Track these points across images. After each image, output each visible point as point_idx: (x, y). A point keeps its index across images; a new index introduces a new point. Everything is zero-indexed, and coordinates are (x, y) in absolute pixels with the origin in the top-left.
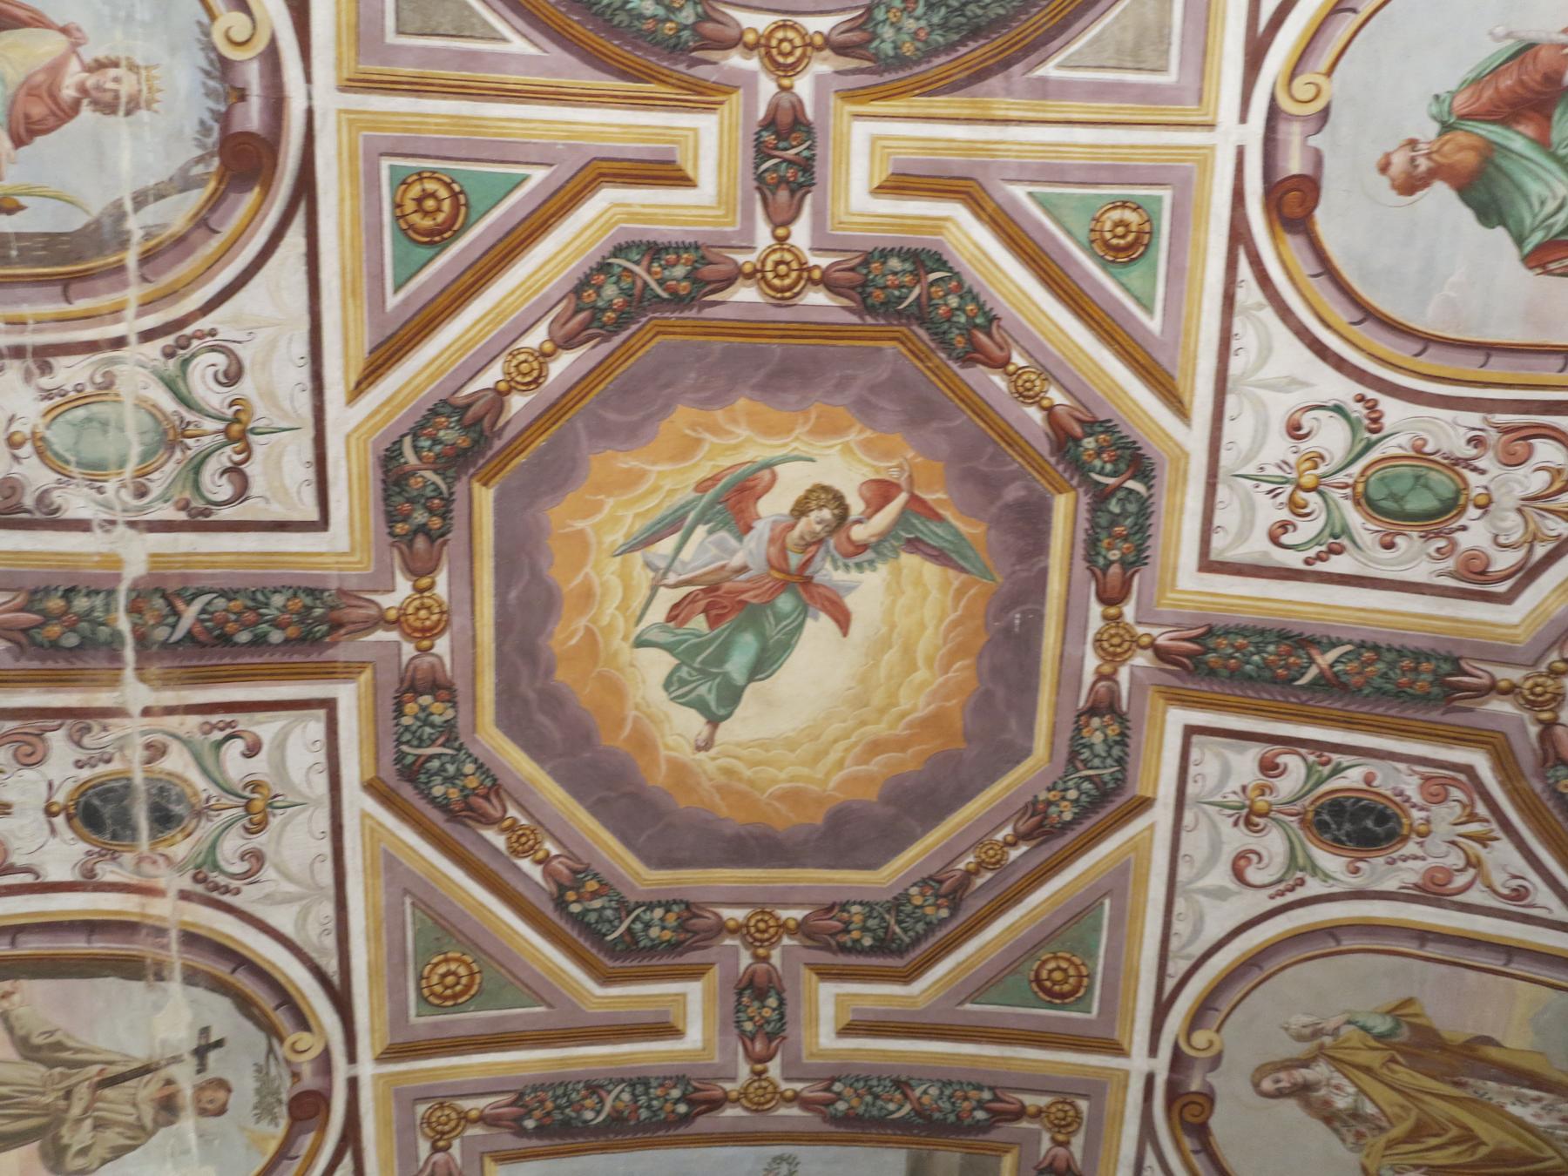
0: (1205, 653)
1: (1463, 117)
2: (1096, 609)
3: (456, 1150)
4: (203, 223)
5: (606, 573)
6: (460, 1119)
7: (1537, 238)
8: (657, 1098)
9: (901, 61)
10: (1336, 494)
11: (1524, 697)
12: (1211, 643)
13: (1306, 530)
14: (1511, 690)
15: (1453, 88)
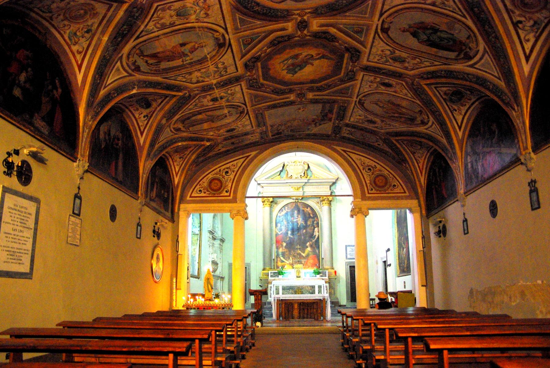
2: (351, 64)
4: (217, 53)
5: (278, 66)
9: (322, 14)
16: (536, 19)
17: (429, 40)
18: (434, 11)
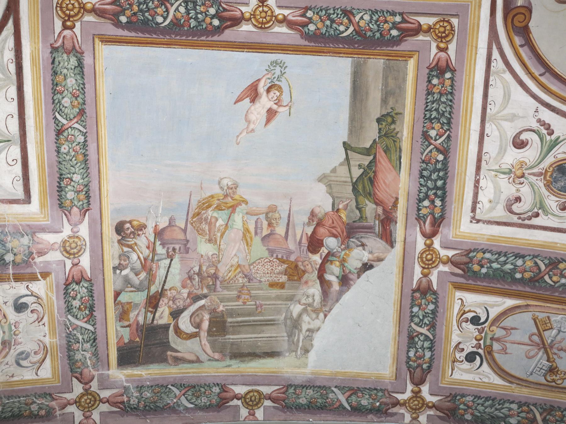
3: (77, 30)
6: (80, 8)
8: (201, 13)
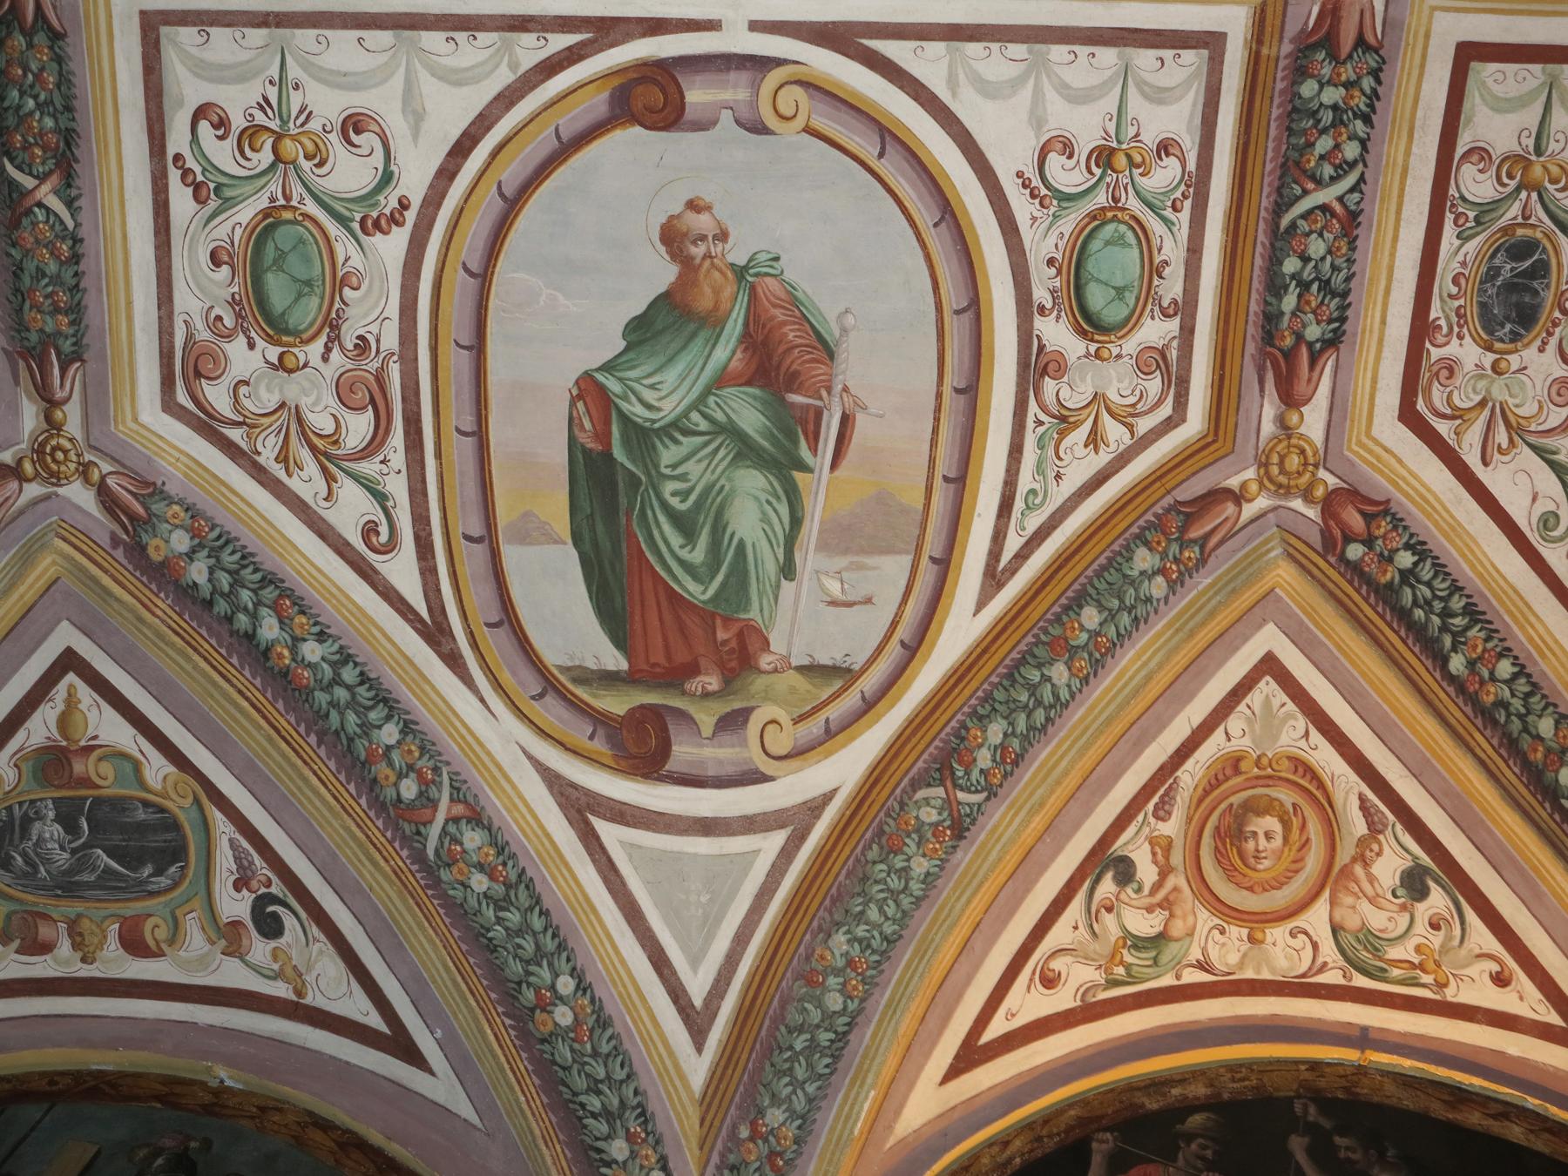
0: (23, 31)
1: (753, 288)
7: (613, 385)
10: (275, 187)
11: (46, 440)
12: (41, 39)
13: (222, 154)
14: (53, 425)
15: (787, 276)
16: (1178, 928)
17: (642, 438)
18: (972, 391)
